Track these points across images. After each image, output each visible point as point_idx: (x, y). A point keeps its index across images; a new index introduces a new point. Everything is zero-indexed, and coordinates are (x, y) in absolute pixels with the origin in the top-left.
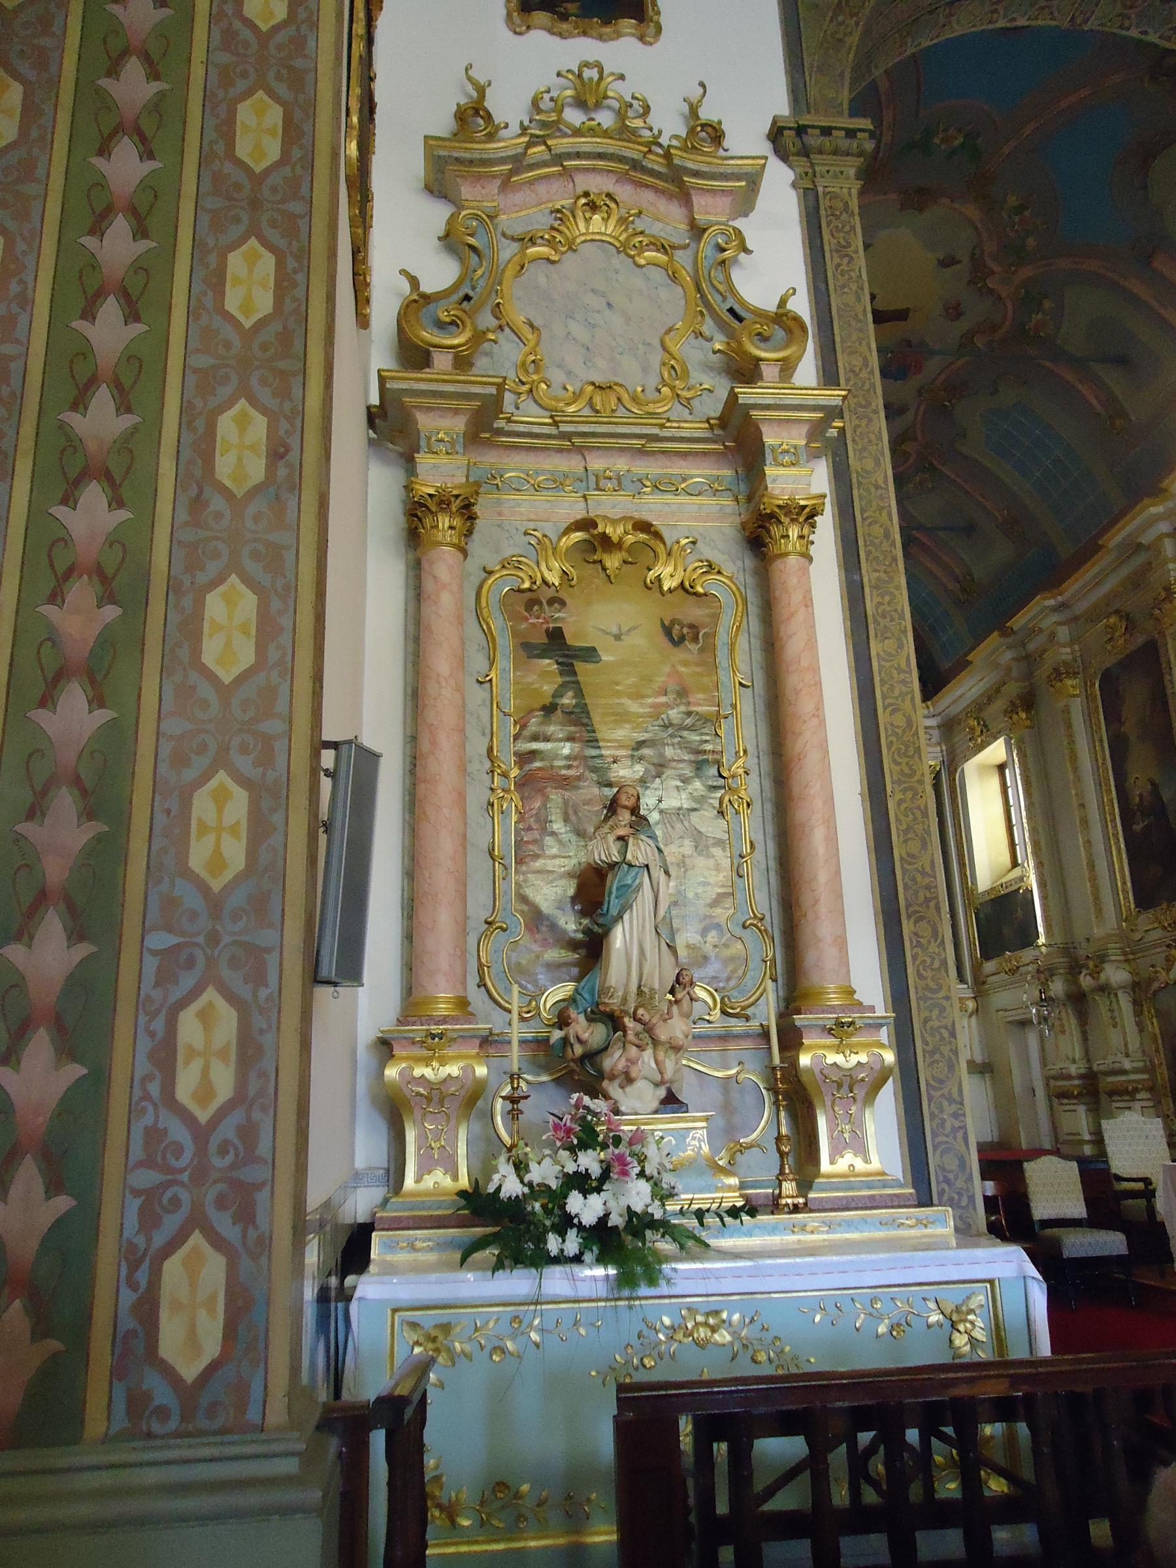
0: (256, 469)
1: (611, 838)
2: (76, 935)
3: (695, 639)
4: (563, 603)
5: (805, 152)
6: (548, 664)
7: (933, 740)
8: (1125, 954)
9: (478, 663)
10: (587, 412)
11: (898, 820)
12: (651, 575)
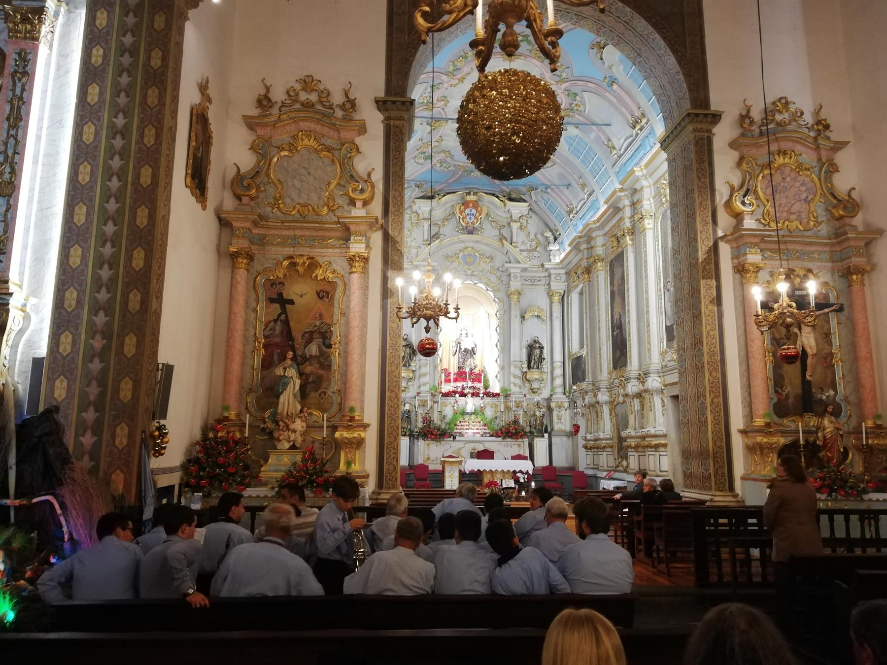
0: (138, 307)
1: (281, 368)
2: (96, 411)
3: (328, 297)
4: (283, 284)
5: (386, 110)
6: (277, 305)
7: (562, 280)
9: (254, 304)
10: (298, 215)
11: (389, 359)
12: (314, 275)
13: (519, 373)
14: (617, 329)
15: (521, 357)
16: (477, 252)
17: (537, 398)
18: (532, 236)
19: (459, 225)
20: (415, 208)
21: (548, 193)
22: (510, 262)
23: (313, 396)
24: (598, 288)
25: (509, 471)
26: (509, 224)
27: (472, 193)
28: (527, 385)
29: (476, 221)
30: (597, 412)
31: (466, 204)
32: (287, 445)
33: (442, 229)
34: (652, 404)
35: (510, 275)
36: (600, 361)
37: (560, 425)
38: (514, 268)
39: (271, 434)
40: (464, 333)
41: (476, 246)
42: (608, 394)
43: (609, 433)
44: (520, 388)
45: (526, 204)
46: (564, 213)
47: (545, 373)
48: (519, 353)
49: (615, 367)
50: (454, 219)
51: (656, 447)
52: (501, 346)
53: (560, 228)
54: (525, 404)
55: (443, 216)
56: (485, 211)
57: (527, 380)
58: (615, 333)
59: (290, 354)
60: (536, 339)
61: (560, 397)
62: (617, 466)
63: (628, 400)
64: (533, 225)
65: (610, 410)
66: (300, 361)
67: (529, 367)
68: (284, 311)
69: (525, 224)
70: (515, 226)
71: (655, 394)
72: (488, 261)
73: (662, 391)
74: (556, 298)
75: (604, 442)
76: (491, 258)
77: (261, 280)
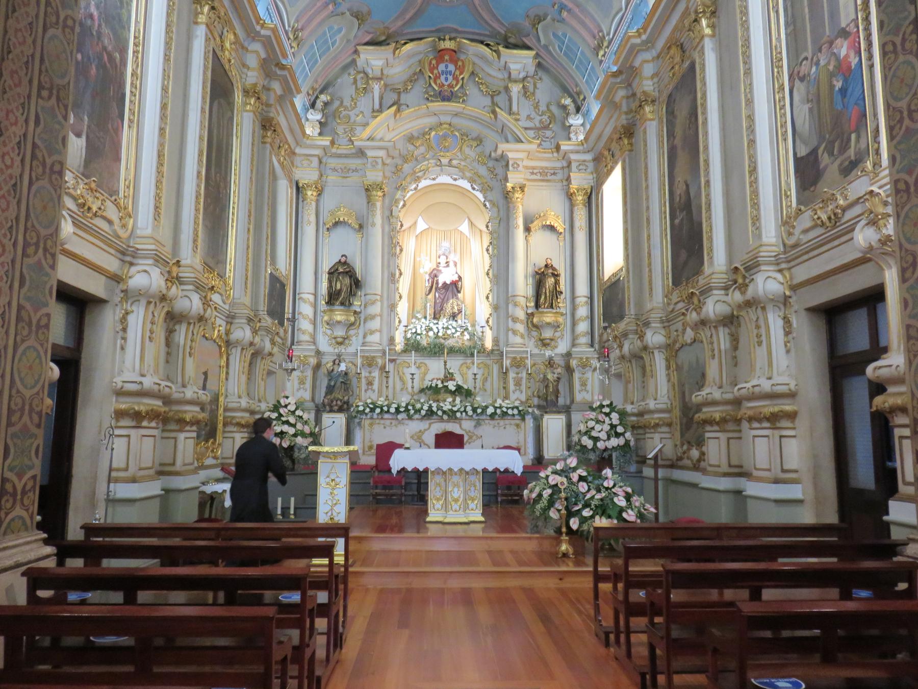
7: (589, 170)
8: (662, 322)
14: (682, 210)
16: (458, 130)
17: (548, 353)
18: (543, 107)
19: (430, 89)
20: (361, 62)
21: (562, 21)
24: (646, 152)
25: (461, 470)
26: (507, 89)
27: (447, 37)
28: (535, 334)
29: (454, 83)
30: (644, 368)
31: (440, 54)
33: (403, 96)
34: (763, 331)
35: (507, 165)
36: (650, 277)
37: (584, 394)
38: (513, 152)
40: (443, 260)
41: (456, 121)
42: (663, 332)
43: (665, 399)
44: (522, 336)
45: (534, 52)
46: (589, 54)
47: (562, 314)
48: (522, 286)
49: (676, 282)
50: (421, 82)
51: (773, 419)
52: (494, 275)
53: (583, 87)
54: (529, 362)
55: (405, 77)
56: (469, 69)
57: (535, 326)
58: (677, 221)
60: (549, 261)
61: (584, 349)
62: (680, 459)
63: (705, 334)
64: (545, 90)
65: (667, 360)
67: (537, 306)
69: (531, 89)
70: (515, 89)
71: (770, 308)
72: (475, 144)
73: (786, 300)
74: (580, 198)
75: (656, 416)
76: (479, 140)
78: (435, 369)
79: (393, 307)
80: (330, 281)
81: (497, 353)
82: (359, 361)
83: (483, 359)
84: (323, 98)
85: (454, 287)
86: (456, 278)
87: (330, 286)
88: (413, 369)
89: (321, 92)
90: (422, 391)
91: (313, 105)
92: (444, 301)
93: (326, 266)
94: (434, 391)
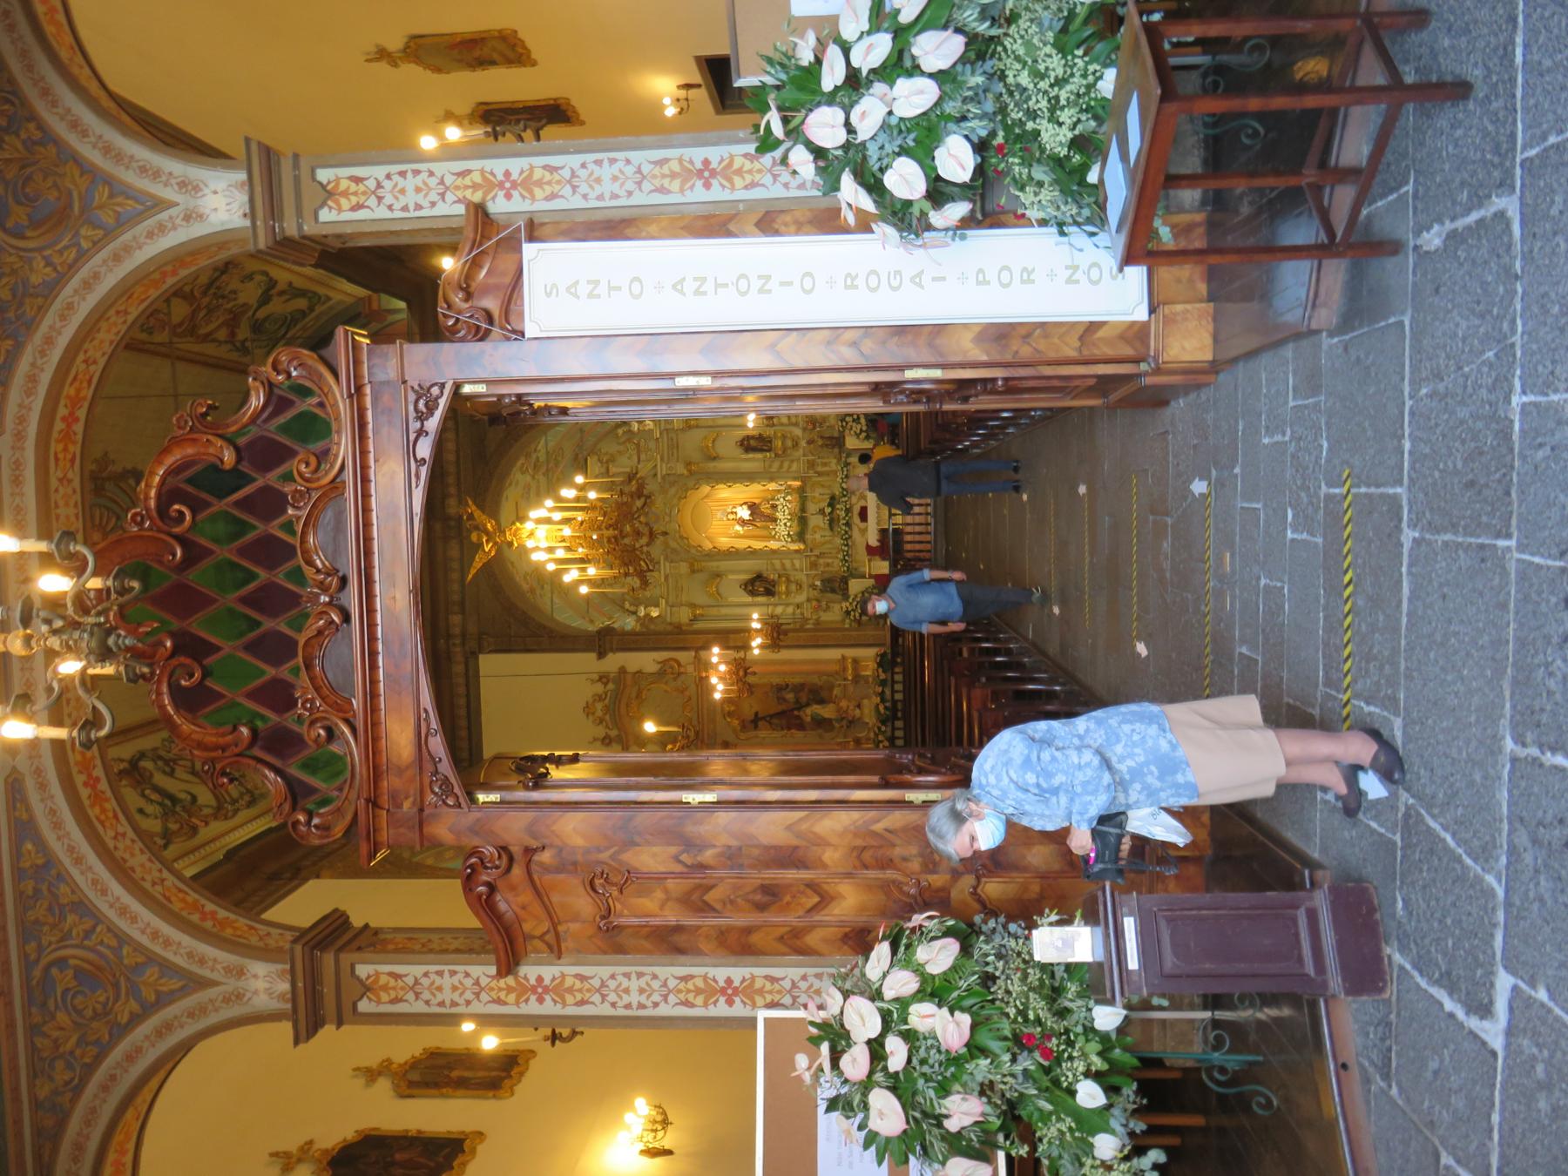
13: (776, 465)
15: (758, 460)
17: (803, 443)
18: (621, 448)
22: (655, 475)
23: (824, 694)
32: (857, 712)
38: (662, 469)
39: (851, 722)
40: (731, 517)
44: (792, 461)
48: (754, 462)
54: (811, 458)
59: (796, 713)
66: (800, 706)
67: (769, 450)
68: (763, 718)
77: (743, 736)
78: (816, 521)
79: (774, 552)
80: (758, 595)
81: (804, 480)
82: (813, 572)
83: (808, 489)
84: (627, 605)
85: (753, 507)
86: (745, 507)
87: (762, 595)
88: (817, 536)
89: (622, 607)
90: (831, 529)
91: (635, 613)
92: (762, 514)
93: (749, 599)
94: (832, 523)
